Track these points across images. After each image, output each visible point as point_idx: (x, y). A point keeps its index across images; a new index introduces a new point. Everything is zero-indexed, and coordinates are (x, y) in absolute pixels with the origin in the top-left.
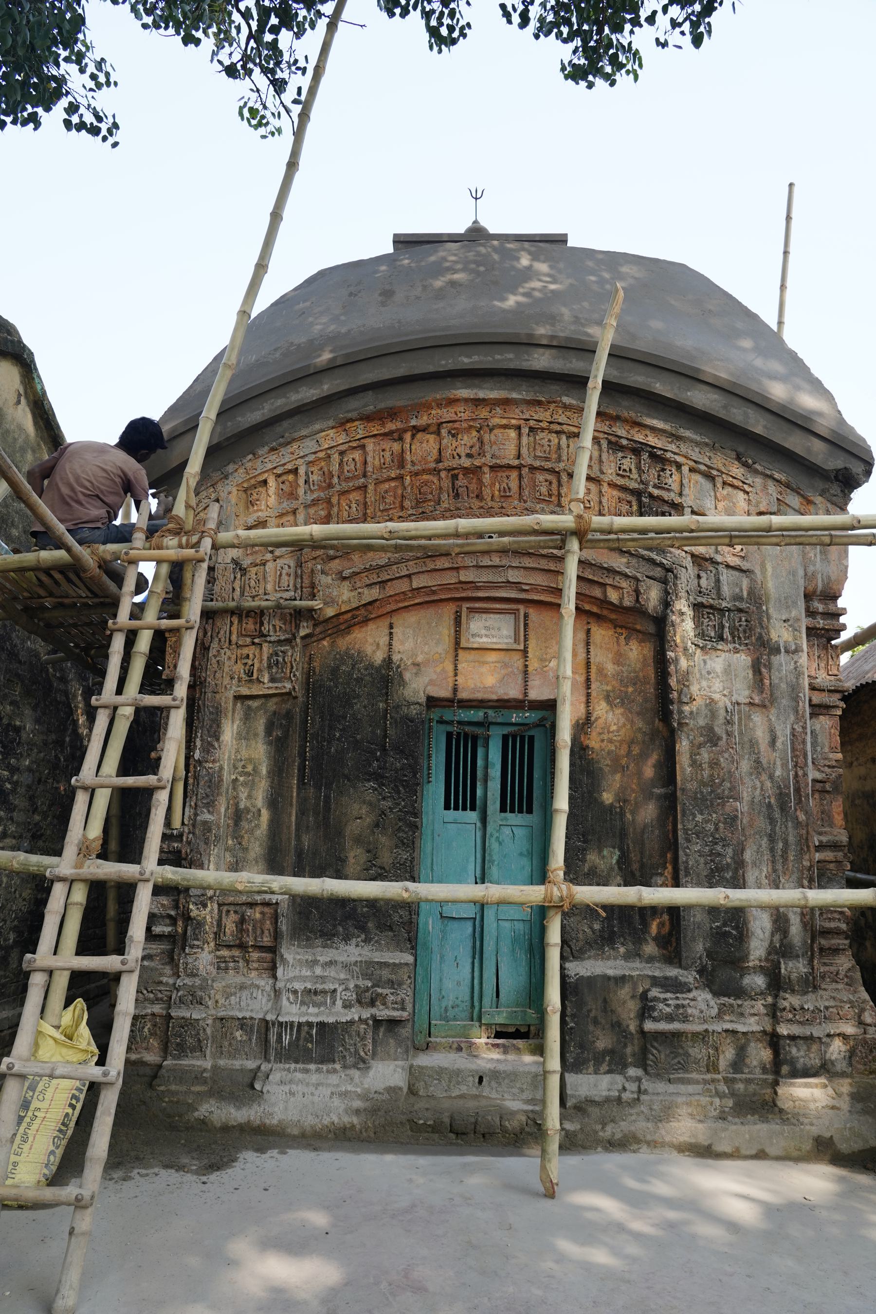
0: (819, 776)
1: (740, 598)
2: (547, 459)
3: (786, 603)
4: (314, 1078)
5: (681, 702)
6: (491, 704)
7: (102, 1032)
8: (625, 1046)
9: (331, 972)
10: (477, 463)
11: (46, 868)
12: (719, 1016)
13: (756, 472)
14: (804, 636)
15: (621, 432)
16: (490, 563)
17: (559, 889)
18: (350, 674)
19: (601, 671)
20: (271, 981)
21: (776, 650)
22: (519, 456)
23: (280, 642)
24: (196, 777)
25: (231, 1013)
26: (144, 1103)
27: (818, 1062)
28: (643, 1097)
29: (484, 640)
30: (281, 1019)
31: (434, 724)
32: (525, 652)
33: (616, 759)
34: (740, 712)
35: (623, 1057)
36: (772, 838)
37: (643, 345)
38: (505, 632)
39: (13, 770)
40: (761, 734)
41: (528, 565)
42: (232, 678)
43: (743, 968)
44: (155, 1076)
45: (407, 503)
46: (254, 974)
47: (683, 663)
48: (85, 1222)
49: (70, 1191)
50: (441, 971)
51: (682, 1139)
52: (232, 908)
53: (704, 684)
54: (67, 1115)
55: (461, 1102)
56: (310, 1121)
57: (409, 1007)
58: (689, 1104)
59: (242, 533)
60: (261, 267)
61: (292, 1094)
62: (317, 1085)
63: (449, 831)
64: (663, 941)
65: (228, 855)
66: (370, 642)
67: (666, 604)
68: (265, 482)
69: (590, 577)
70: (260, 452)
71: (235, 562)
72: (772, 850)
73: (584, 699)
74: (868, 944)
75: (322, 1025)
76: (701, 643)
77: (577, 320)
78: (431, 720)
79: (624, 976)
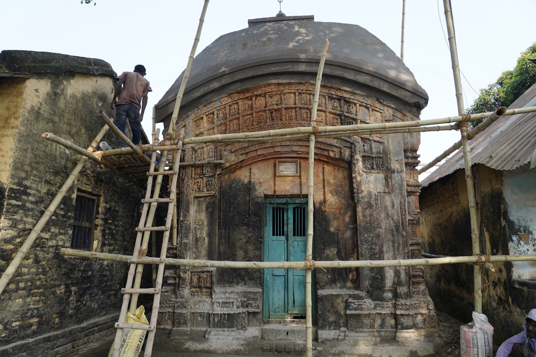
0: (411, 218)
1: (379, 153)
2: (306, 104)
3: (397, 154)
4: (227, 333)
5: (358, 193)
7: (148, 312)
8: (340, 320)
9: (232, 296)
12: (375, 308)
13: (384, 105)
15: (333, 93)
17: (310, 262)
18: (236, 187)
20: (210, 299)
21: (394, 172)
22: (295, 104)
23: (210, 176)
24: (181, 226)
25: (196, 311)
27: (412, 324)
28: (346, 338)
29: (285, 173)
30: (214, 313)
31: (267, 204)
32: (300, 176)
33: (335, 215)
34: (380, 195)
35: (339, 324)
36: (393, 242)
37: (341, 59)
38: (292, 170)
39: (116, 226)
40: (388, 203)
42: (193, 190)
43: (383, 290)
44: (170, 334)
45: (254, 123)
46: (204, 297)
47: (359, 178)
50: (273, 295)
51: (360, 352)
52: (195, 273)
53: (367, 185)
56: (225, 348)
57: (261, 307)
58: (363, 340)
59: (193, 138)
60: (197, 40)
61: (219, 339)
62: (228, 336)
63: (274, 243)
64: (353, 281)
65: (193, 254)
66: (243, 175)
67: (352, 156)
68: (202, 118)
70: (200, 107)
71: (192, 148)
72: (393, 246)
73: (323, 193)
74: (442, 282)
75: (229, 314)
76: (365, 170)
77: (315, 51)
79: (339, 295)
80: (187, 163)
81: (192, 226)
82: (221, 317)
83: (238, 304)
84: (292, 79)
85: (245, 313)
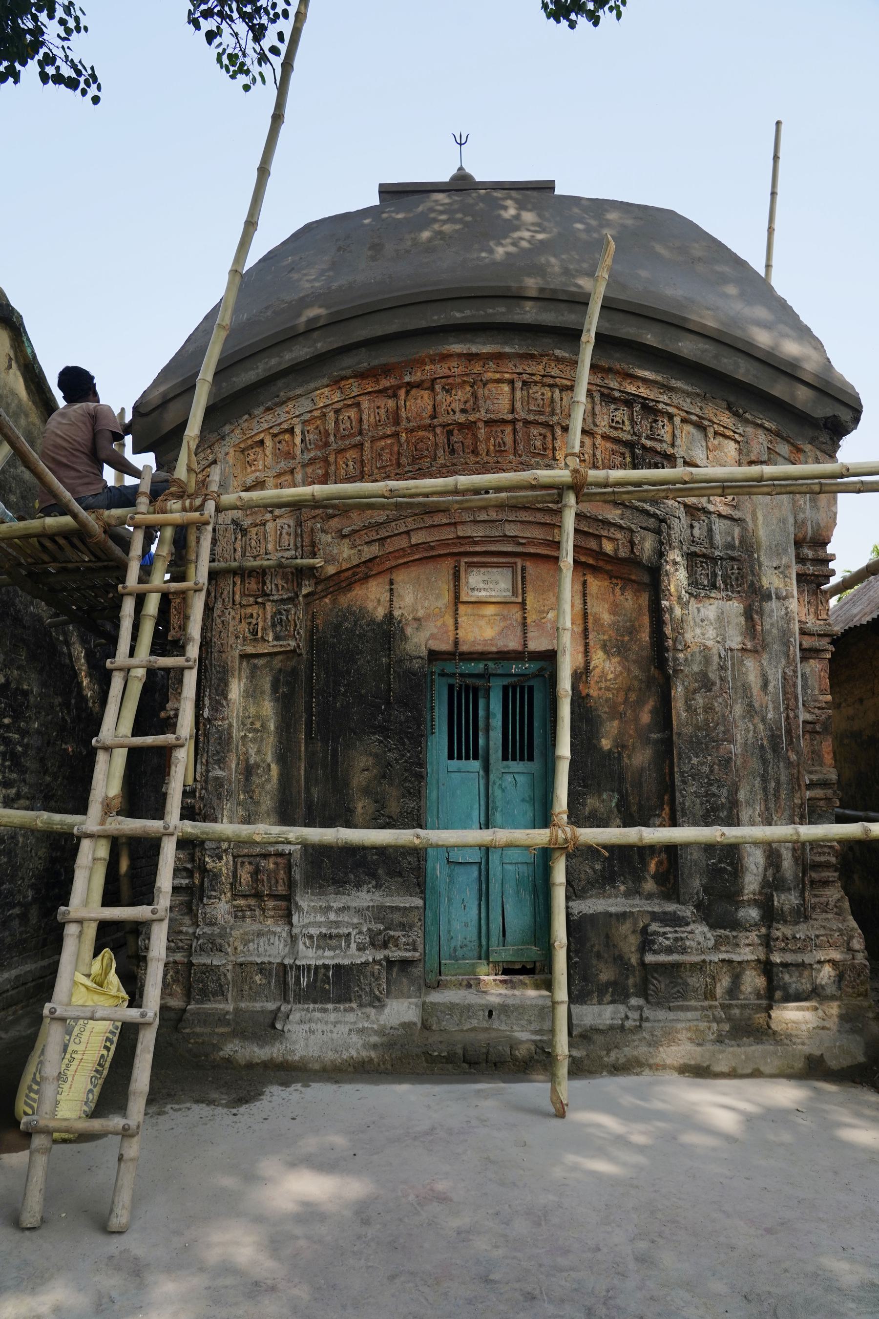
0: (809, 717)
2: (541, 413)
3: (777, 551)
4: (332, 1017)
5: (676, 650)
6: (490, 656)
8: (627, 978)
9: (345, 917)
10: (472, 418)
11: (73, 826)
13: (747, 422)
14: (795, 582)
15: (613, 384)
17: (564, 831)
19: (597, 621)
21: (768, 597)
22: (513, 410)
23: (282, 601)
25: (250, 959)
26: (171, 1045)
27: (809, 987)
28: (645, 1024)
29: (483, 593)
30: (298, 963)
31: (435, 677)
32: (523, 604)
33: (614, 707)
34: (732, 657)
36: (765, 779)
38: (502, 585)
39: (24, 733)
40: (753, 678)
41: (524, 519)
42: (237, 637)
43: (738, 902)
44: (180, 1020)
45: (404, 460)
46: (270, 921)
47: (678, 611)
48: (132, 1149)
49: (116, 1122)
50: (449, 913)
52: (246, 860)
53: (698, 631)
54: (102, 1056)
55: (473, 1035)
56: (330, 1056)
57: (420, 948)
58: (689, 1029)
60: (251, 225)
61: (312, 1032)
62: (335, 1024)
63: (453, 778)
64: (661, 878)
65: (240, 809)
66: (372, 598)
68: (262, 442)
70: (256, 412)
71: (234, 522)
72: (765, 789)
74: (856, 877)
75: (337, 967)
77: (566, 272)
78: (432, 673)
79: (625, 912)
80: (223, 565)
81: (237, 734)
82: (316, 974)
83: (361, 939)
84: (505, 343)
85: (379, 963)
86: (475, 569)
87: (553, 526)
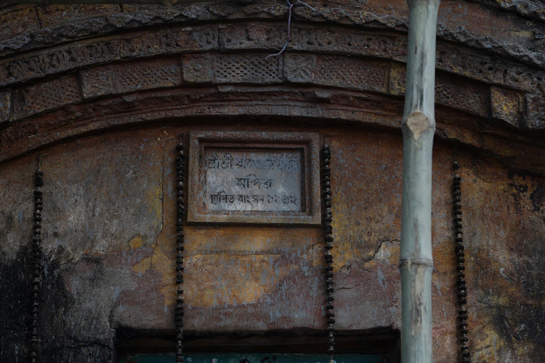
16: (247, 45)
19: (484, 264)
29: (239, 206)
32: (324, 230)
38: (281, 190)
41: (326, 47)
69: (457, 70)
86: (221, 155)
87: (387, 63)
